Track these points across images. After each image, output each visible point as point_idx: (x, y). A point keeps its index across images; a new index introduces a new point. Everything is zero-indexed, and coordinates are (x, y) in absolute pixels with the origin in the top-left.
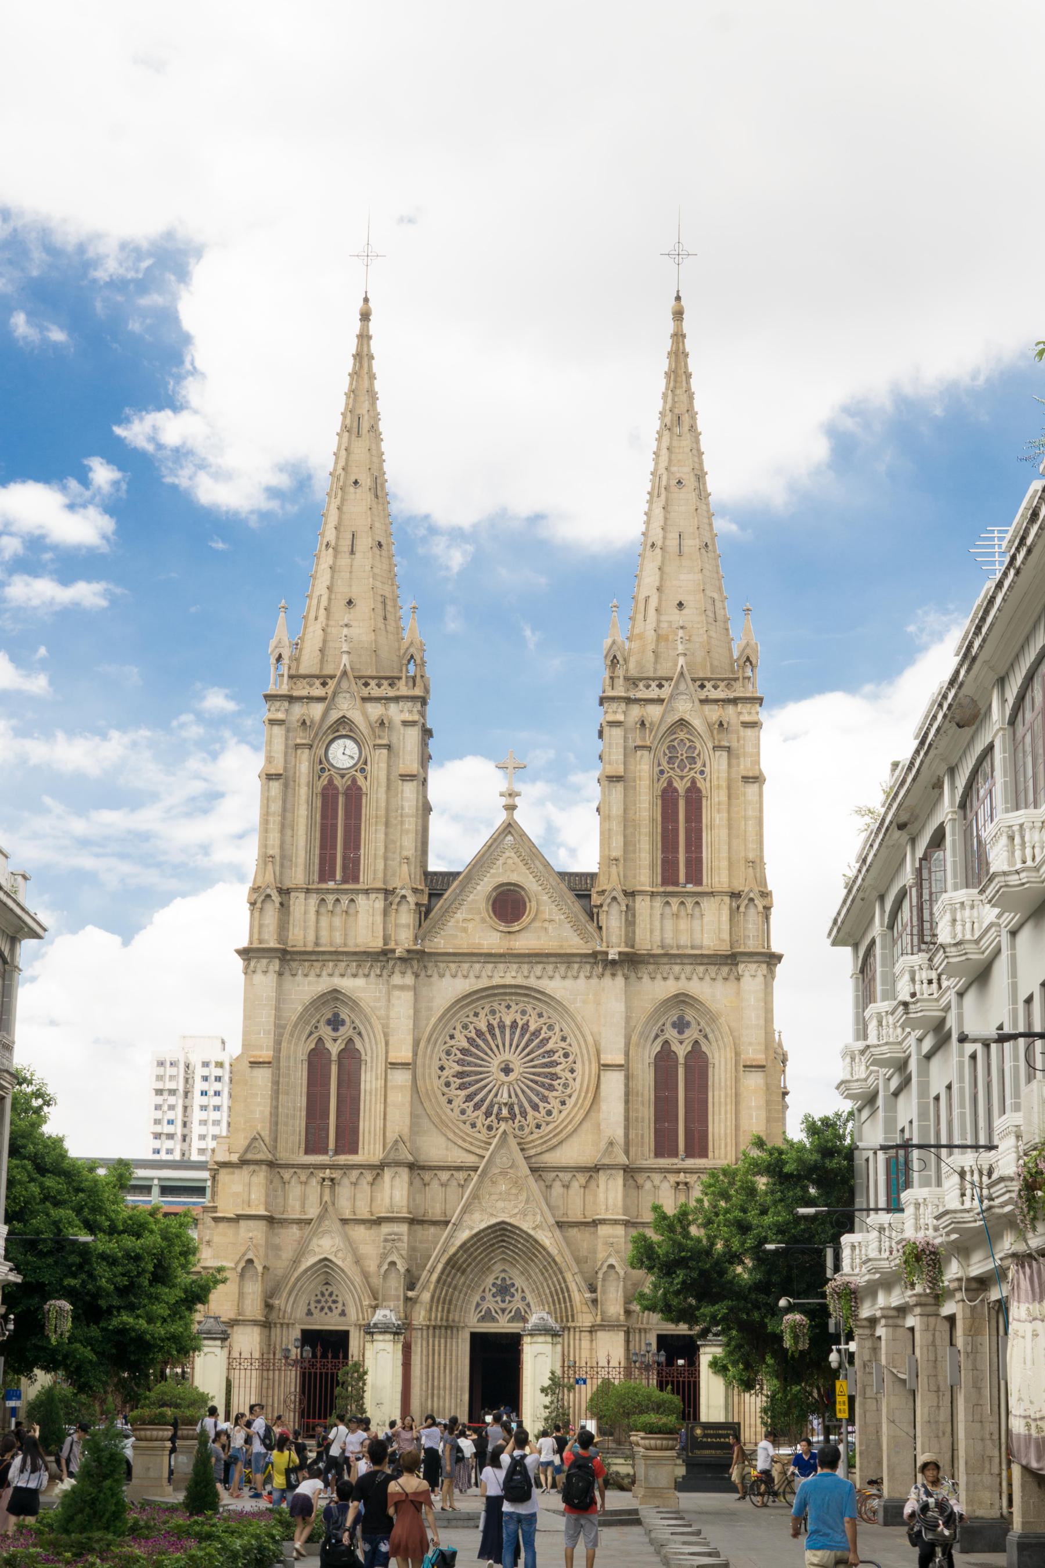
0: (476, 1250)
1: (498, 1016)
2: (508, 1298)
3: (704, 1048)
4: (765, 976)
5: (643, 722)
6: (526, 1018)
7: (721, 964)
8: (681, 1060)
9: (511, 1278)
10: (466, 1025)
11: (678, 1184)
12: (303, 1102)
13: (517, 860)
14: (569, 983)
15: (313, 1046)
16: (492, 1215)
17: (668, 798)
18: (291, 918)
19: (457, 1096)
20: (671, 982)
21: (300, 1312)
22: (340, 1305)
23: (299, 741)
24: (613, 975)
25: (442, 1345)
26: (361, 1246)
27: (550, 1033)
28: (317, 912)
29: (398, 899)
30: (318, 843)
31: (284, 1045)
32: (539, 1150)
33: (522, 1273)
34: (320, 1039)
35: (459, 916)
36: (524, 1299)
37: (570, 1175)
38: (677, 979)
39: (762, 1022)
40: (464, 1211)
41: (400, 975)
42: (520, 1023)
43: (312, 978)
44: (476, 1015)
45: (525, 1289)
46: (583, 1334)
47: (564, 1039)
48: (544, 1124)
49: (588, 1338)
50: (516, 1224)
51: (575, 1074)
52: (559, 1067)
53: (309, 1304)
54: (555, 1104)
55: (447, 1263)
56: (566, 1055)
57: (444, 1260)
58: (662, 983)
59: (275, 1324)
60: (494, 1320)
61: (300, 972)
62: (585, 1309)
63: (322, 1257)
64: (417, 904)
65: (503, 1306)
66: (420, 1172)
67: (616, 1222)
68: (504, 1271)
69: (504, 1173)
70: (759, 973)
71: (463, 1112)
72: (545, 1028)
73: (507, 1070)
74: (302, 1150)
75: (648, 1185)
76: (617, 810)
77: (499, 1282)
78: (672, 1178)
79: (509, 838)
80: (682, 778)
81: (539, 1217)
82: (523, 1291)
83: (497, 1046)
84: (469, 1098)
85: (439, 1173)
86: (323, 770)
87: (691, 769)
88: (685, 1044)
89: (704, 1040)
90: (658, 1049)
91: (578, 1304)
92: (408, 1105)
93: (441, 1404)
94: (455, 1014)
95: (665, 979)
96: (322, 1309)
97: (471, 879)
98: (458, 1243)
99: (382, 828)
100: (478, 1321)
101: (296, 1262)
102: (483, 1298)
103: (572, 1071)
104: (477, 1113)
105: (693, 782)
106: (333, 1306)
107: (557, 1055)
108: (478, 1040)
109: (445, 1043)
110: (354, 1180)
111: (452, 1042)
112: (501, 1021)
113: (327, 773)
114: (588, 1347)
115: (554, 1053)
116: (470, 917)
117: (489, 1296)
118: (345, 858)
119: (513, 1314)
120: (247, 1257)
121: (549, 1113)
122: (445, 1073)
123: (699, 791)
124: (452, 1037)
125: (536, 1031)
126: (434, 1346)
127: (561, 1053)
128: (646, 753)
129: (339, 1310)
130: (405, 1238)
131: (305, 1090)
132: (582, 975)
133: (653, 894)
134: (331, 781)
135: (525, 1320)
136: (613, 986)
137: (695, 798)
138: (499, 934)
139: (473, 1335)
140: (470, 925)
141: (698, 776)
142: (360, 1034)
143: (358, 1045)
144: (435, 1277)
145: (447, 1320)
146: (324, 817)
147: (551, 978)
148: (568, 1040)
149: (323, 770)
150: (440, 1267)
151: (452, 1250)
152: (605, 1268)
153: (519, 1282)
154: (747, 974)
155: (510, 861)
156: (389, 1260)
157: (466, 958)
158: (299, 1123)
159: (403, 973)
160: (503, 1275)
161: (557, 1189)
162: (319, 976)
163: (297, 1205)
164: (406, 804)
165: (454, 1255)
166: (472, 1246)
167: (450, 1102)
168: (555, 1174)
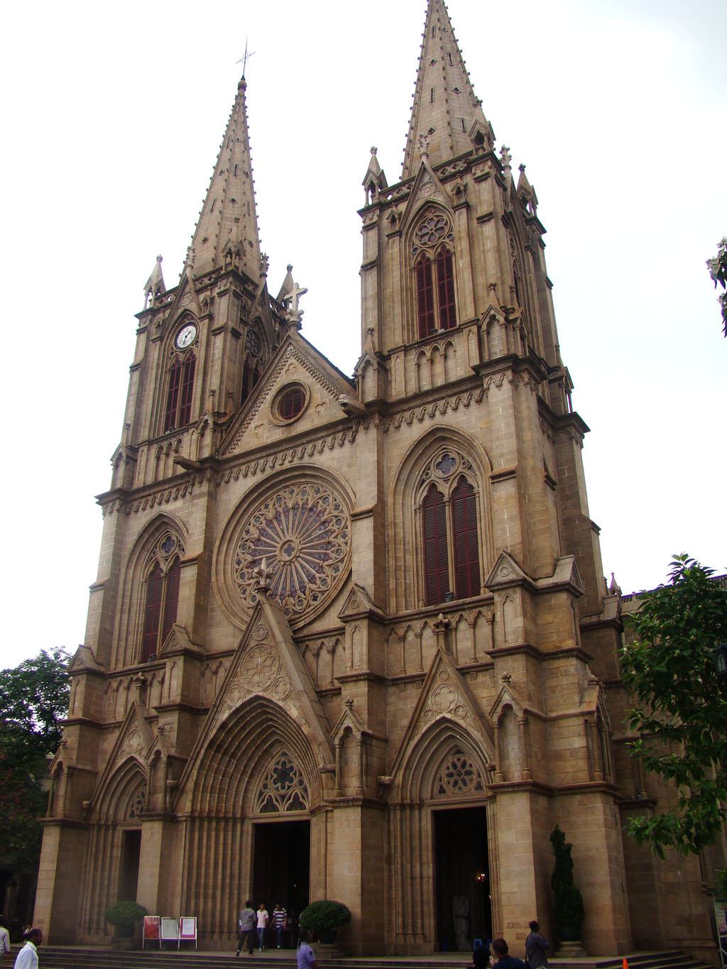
0: (243, 728)
1: (283, 502)
2: (287, 783)
3: (470, 481)
4: (511, 382)
5: (393, 215)
6: (305, 498)
7: (472, 389)
8: (446, 498)
9: (290, 762)
11: (437, 626)
13: (296, 363)
14: (338, 451)
15: (151, 569)
16: (249, 691)
17: (422, 270)
18: (138, 467)
19: (249, 585)
23: (154, 337)
24: (367, 428)
25: (213, 839)
27: (325, 506)
28: (158, 458)
29: (202, 424)
30: (165, 406)
31: (123, 570)
32: (308, 620)
34: (157, 564)
35: (252, 425)
36: (301, 782)
37: (334, 639)
39: (513, 429)
41: (199, 485)
42: (301, 503)
43: (148, 510)
44: (267, 507)
45: (303, 773)
46: (329, 815)
48: (319, 594)
51: (347, 538)
52: (334, 535)
55: (210, 746)
56: (339, 521)
57: (205, 746)
59: (94, 825)
60: (275, 809)
61: (140, 509)
64: (215, 423)
65: (283, 792)
66: (208, 661)
67: (356, 679)
68: (284, 754)
70: (506, 382)
72: (321, 502)
73: (289, 551)
74: (136, 661)
75: (411, 636)
76: (372, 290)
77: (280, 767)
78: (432, 622)
79: (291, 347)
80: (432, 247)
82: (301, 775)
83: (282, 530)
86: (173, 353)
87: (439, 238)
88: (450, 482)
89: (469, 472)
90: (425, 494)
92: (193, 598)
93: (210, 904)
94: (245, 510)
95: (421, 420)
97: (260, 392)
98: (218, 725)
99: (201, 377)
100: (261, 811)
101: (111, 763)
102: (265, 786)
105: (443, 246)
107: (331, 524)
108: (267, 529)
109: (243, 539)
110: (160, 679)
113: (174, 355)
116: (259, 423)
118: (182, 410)
119: (291, 801)
121: (324, 580)
122: (241, 566)
123: (448, 251)
124: (248, 532)
125: (313, 506)
126: (200, 839)
128: (397, 238)
130: (176, 726)
131: (143, 607)
132: (346, 442)
133: (406, 349)
134: (177, 361)
135: (302, 806)
136: (367, 439)
137: (446, 260)
138: (281, 429)
140: (260, 430)
141: (447, 240)
142: (183, 550)
145: (218, 811)
146: (171, 387)
147: (321, 452)
149: (173, 353)
150: (203, 751)
152: (341, 732)
154: (493, 387)
155: (292, 366)
156: (155, 749)
157: (253, 457)
158: (136, 639)
159: (201, 483)
160: (283, 759)
161: (325, 657)
162: (152, 507)
164: (216, 352)
165: (215, 737)
166: (235, 725)
167: (244, 593)
168: (319, 642)
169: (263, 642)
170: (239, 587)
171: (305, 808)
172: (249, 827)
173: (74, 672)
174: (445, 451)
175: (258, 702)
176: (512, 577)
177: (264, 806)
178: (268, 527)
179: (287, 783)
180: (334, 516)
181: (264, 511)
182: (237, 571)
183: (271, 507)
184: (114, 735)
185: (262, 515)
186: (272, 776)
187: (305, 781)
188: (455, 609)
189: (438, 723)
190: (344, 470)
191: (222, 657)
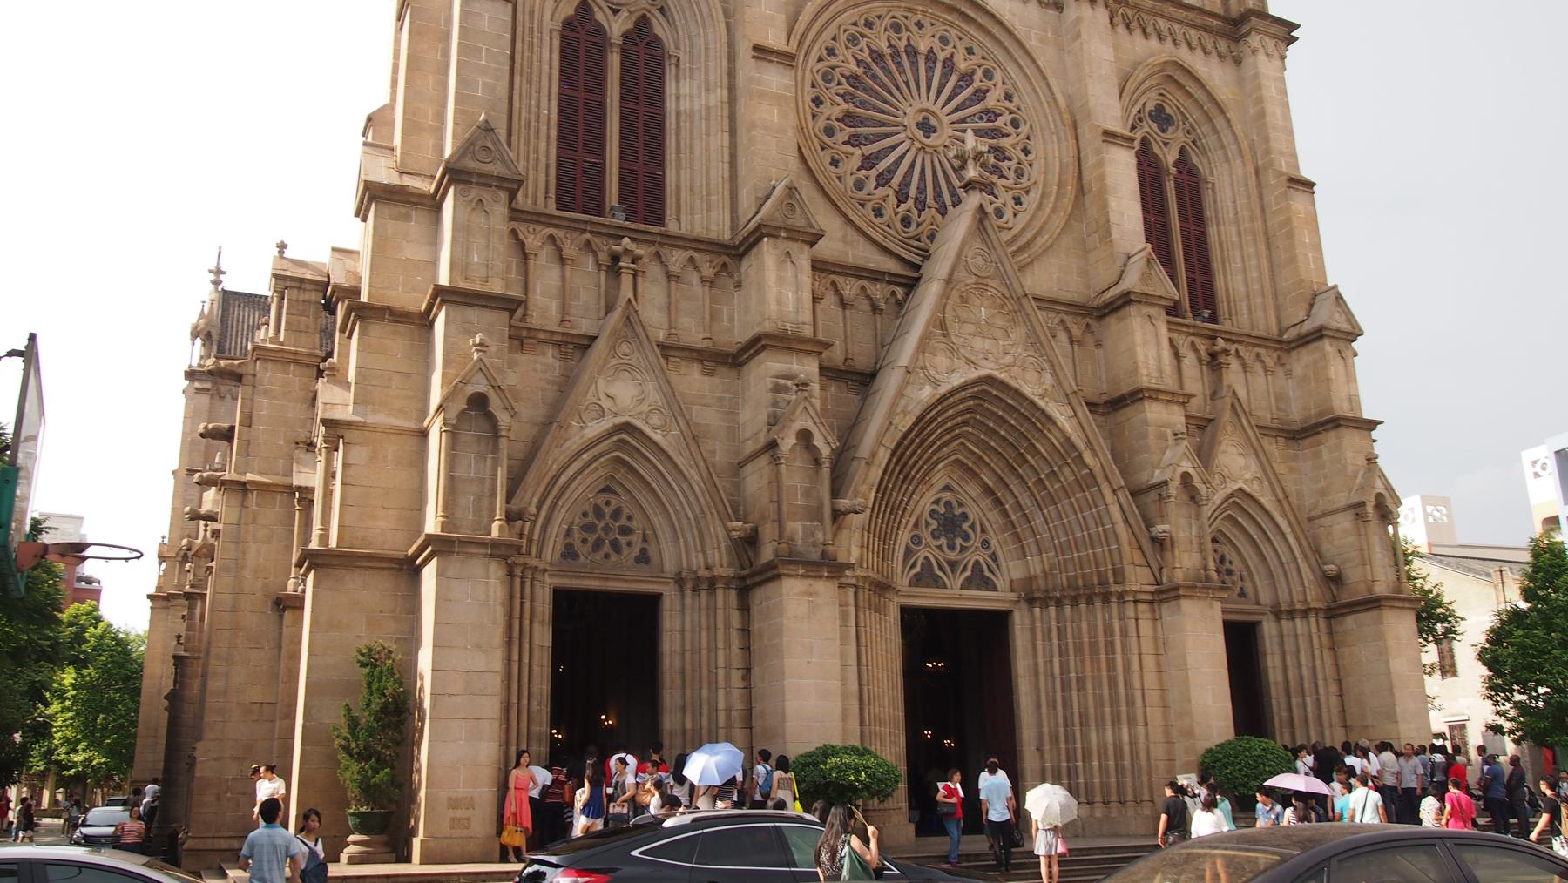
1: (905, 34)
2: (959, 541)
3: (1195, 160)
6: (949, 49)
9: (961, 505)
10: (853, 35)
12: (550, 110)
16: (969, 362)
19: (848, 155)
20: (1154, 42)
21: (552, 550)
22: (636, 538)
26: (696, 409)
33: (989, 491)
36: (986, 544)
38: (1160, 38)
40: (922, 347)
44: (869, 25)
46: (1141, 607)
47: (1008, 97)
49: (1149, 615)
50: (1013, 383)
51: (1031, 157)
53: (568, 533)
54: (1006, 198)
57: (891, 441)
58: (1144, 41)
60: (937, 583)
62: (1138, 558)
63: (619, 420)
65: (952, 555)
68: (947, 488)
69: (981, 286)
71: (859, 185)
72: (979, 73)
81: (1048, 378)
82: (983, 531)
84: (868, 162)
85: (840, 280)
91: (1126, 548)
96: (598, 545)
103: (1026, 151)
104: (881, 192)
106: (623, 540)
111: (833, 61)
112: (909, 45)
114: (1150, 633)
115: (997, 115)
117: (926, 536)
119: (968, 573)
120: (471, 389)
127: (1007, 117)
129: (636, 551)
131: (555, 88)
139: (905, 610)
143: (659, 28)
144: (876, 473)
148: (1016, 99)
151: (905, 423)
153: (973, 512)
156: (798, 425)
163: (554, 306)
169: (989, 281)
170: (823, 149)
171: (995, 589)
172: (894, 615)
173: (470, 173)
174: (1161, 98)
175: (980, 388)
176: (1345, 326)
177: (915, 575)
178: (876, 63)
179: (959, 541)
180: (1006, 108)
181: (867, 31)
182: (814, 116)
183: (879, 27)
184: (539, 359)
185: (863, 36)
186: (927, 524)
187: (994, 542)
188: (1234, 338)
189: (1231, 495)
190: (1034, 42)
191: (839, 274)
